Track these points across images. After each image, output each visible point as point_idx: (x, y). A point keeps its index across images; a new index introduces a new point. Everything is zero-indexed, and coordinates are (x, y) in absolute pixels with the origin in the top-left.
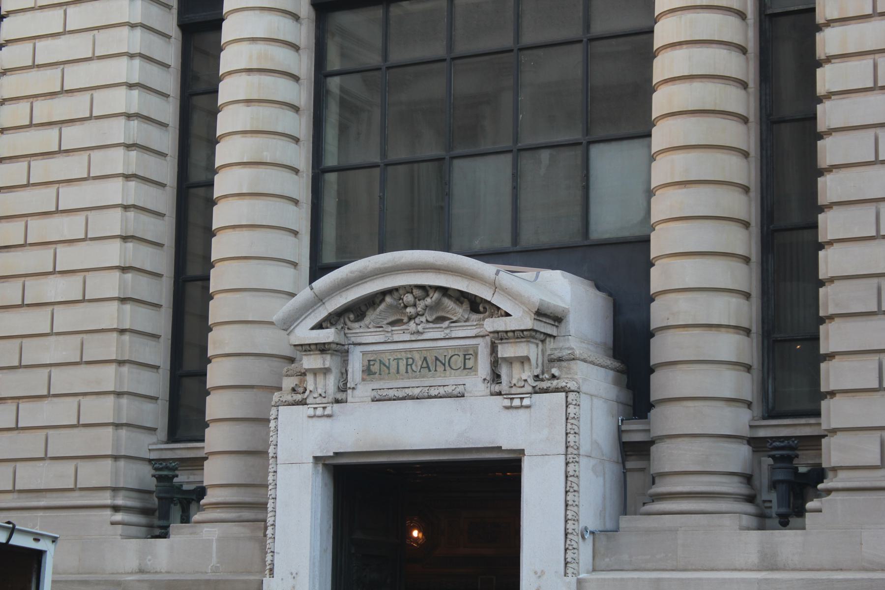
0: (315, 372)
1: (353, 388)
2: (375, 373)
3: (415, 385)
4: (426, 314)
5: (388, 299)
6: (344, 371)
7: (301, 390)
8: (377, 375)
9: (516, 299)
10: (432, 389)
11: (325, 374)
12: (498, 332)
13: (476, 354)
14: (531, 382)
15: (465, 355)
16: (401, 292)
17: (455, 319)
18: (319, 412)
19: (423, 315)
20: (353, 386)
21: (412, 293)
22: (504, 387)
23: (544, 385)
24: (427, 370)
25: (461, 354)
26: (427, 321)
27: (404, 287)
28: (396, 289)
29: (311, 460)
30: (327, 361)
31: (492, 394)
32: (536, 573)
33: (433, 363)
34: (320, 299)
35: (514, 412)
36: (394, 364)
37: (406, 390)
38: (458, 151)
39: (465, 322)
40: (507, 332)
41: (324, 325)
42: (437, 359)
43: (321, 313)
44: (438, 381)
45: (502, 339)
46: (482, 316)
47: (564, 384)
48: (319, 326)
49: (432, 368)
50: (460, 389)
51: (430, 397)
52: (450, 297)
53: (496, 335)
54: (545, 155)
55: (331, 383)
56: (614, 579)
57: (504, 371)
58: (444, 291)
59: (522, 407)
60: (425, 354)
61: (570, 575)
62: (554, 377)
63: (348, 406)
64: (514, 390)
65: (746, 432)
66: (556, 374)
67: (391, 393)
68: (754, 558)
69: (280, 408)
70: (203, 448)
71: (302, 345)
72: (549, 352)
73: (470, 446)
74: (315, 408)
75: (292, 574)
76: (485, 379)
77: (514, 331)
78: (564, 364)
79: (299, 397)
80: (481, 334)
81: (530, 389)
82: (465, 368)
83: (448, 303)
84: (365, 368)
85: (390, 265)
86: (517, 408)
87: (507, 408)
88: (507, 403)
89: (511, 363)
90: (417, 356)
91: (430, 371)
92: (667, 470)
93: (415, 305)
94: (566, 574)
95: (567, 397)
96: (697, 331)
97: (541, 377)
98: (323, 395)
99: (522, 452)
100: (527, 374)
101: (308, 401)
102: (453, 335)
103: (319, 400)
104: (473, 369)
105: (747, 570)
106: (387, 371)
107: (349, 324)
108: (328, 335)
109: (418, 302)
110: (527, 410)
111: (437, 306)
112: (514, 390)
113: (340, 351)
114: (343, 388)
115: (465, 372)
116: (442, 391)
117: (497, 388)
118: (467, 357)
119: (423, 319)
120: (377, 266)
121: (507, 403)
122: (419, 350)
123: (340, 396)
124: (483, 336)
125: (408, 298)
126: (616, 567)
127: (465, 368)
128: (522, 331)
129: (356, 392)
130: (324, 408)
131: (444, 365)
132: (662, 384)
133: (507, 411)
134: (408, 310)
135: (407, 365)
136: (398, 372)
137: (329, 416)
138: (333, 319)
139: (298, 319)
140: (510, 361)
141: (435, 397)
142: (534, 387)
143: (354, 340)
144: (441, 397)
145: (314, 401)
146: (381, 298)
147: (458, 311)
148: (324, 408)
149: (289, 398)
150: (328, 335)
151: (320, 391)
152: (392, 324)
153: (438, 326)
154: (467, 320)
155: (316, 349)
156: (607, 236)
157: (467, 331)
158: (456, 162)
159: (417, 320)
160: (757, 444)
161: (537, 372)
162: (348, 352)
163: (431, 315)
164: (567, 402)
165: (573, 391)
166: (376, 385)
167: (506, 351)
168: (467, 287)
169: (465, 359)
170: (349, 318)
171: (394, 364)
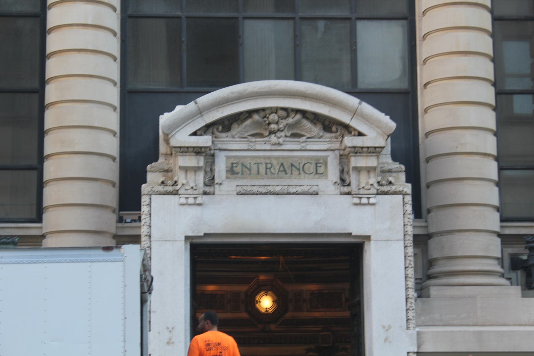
0: (186, 169)
1: (220, 184)
2: (238, 173)
3: (276, 184)
4: (286, 130)
5: (256, 117)
6: (208, 169)
7: (170, 182)
8: (239, 175)
9: (372, 124)
10: (291, 187)
11: (195, 171)
12: (355, 147)
13: (326, 164)
14: (376, 185)
15: (317, 164)
16: (268, 112)
17: (308, 136)
18: (191, 201)
19: (282, 131)
21: (276, 113)
22: (354, 188)
23: (385, 189)
24: (284, 173)
25: (313, 162)
26: (286, 136)
27: (271, 108)
28: (263, 110)
29: (183, 239)
30: (201, 161)
31: (341, 194)
32: (384, 327)
33: (288, 168)
34: (200, 112)
35: (362, 207)
36: (254, 168)
37: (268, 187)
38: (249, 14)
39: (319, 138)
40: (362, 148)
41: (199, 133)
42: (292, 165)
43: (200, 123)
44: (295, 182)
45: (356, 153)
46: (334, 135)
47: (401, 189)
48: (195, 134)
49: (289, 172)
50: (315, 189)
51: (289, 194)
52: (307, 118)
53: (353, 149)
54: (321, 24)
55: (201, 177)
56: (445, 332)
57: (353, 178)
58: (304, 113)
59: (369, 204)
60: (281, 161)
61: (412, 329)
62: (390, 183)
63: (216, 198)
64: (362, 191)
65: (497, 229)
66: (393, 181)
67: (255, 189)
69: (153, 197)
70: (41, 228)
71: (180, 147)
72: (381, 166)
73: (322, 232)
74: (187, 198)
75: (168, 328)
76: (335, 183)
77: (368, 148)
78: (394, 174)
79: (170, 189)
80: (332, 148)
81: (375, 191)
82: (316, 173)
83: (307, 124)
84: (229, 169)
85: (266, 90)
86: (364, 205)
87: (356, 204)
88: (356, 201)
89: (359, 171)
90: (275, 162)
91: (286, 174)
92: (458, 254)
93: (277, 123)
94: (408, 328)
95: (404, 198)
96: (478, 157)
97: (381, 183)
98: (195, 188)
99: (368, 238)
100: (373, 180)
101: (180, 192)
102: (309, 147)
103: (190, 192)
104: (324, 175)
105: (530, 325)
106: (249, 172)
107: (217, 134)
108: (205, 141)
109: (281, 121)
110: (372, 207)
112: (362, 191)
114: (211, 182)
115: (317, 176)
116: (299, 189)
117: (346, 189)
118: (318, 165)
119: (283, 134)
120: (255, 90)
121: (356, 201)
122: (277, 158)
123: (207, 189)
124: (332, 150)
125: (273, 117)
126: (430, 323)
127: (316, 173)
128: (375, 148)
129: (222, 187)
130: (195, 198)
131: (299, 170)
133: (355, 207)
134: (273, 126)
135: (266, 168)
136: (258, 173)
137: (200, 205)
138: (207, 129)
139: (179, 126)
140: (358, 170)
141: (293, 194)
142: (378, 190)
143: (220, 146)
144: (298, 194)
145: (186, 192)
146: (247, 115)
147: (316, 130)
148: (195, 198)
149: (161, 188)
150: (205, 141)
151: (192, 184)
152: (253, 135)
153: (296, 140)
154: (321, 137)
155: (193, 152)
156: (372, 87)
157: (321, 145)
158: (247, 22)
159: (279, 134)
160: (506, 240)
161: (379, 179)
162: (213, 155)
163: (288, 131)
164: (404, 202)
165: (408, 194)
166: (240, 182)
168: (329, 111)
169: (317, 167)
170: (217, 129)
171: (254, 168)
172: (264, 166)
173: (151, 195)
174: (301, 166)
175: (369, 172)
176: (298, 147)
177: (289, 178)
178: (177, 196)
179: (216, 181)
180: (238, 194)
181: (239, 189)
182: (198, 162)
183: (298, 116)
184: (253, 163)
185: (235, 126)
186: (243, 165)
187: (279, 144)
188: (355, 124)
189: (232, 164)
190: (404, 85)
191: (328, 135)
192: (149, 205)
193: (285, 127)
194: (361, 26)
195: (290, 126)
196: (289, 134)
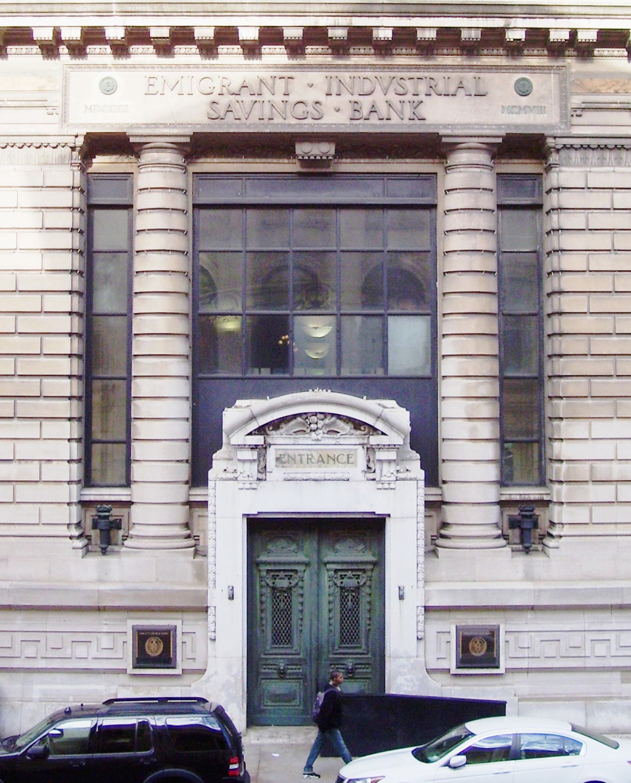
1: (271, 472)
5: (299, 419)
15: (348, 455)
16: (309, 415)
17: (342, 433)
18: (248, 486)
20: (271, 471)
26: (324, 433)
28: (305, 413)
30: (254, 455)
31: (368, 480)
39: (350, 435)
41: (253, 433)
42: (329, 456)
43: (254, 426)
45: (380, 449)
52: (341, 419)
53: (377, 446)
55: (255, 467)
58: (339, 416)
68: (521, 574)
71: (239, 445)
88: (380, 486)
91: (324, 462)
93: (316, 423)
95: (417, 484)
98: (250, 476)
102: (342, 442)
108: (258, 440)
111: (333, 423)
112: (384, 478)
113: (260, 449)
117: (371, 476)
119: (321, 431)
123: (260, 476)
125: (314, 419)
127: (348, 463)
131: (334, 460)
132: (446, 471)
135: (308, 459)
138: (261, 430)
147: (347, 428)
149: (224, 475)
163: (325, 429)
166: (288, 470)
167: (381, 455)
171: (298, 458)
172: (306, 456)
173: (215, 481)
174: (336, 456)
175: (390, 462)
176: (334, 442)
177: (325, 467)
178: (236, 482)
179: (268, 470)
180: (285, 480)
181: (286, 476)
182: (253, 456)
183: (334, 419)
184: (297, 454)
185: (283, 425)
186: (289, 456)
187: (318, 440)
188: (379, 426)
189: (281, 455)
190: (427, 372)
191: (359, 432)
192: (215, 488)
193: (323, 426)
194: (391, 319)
195: (327, 425)
196: (326, 432)
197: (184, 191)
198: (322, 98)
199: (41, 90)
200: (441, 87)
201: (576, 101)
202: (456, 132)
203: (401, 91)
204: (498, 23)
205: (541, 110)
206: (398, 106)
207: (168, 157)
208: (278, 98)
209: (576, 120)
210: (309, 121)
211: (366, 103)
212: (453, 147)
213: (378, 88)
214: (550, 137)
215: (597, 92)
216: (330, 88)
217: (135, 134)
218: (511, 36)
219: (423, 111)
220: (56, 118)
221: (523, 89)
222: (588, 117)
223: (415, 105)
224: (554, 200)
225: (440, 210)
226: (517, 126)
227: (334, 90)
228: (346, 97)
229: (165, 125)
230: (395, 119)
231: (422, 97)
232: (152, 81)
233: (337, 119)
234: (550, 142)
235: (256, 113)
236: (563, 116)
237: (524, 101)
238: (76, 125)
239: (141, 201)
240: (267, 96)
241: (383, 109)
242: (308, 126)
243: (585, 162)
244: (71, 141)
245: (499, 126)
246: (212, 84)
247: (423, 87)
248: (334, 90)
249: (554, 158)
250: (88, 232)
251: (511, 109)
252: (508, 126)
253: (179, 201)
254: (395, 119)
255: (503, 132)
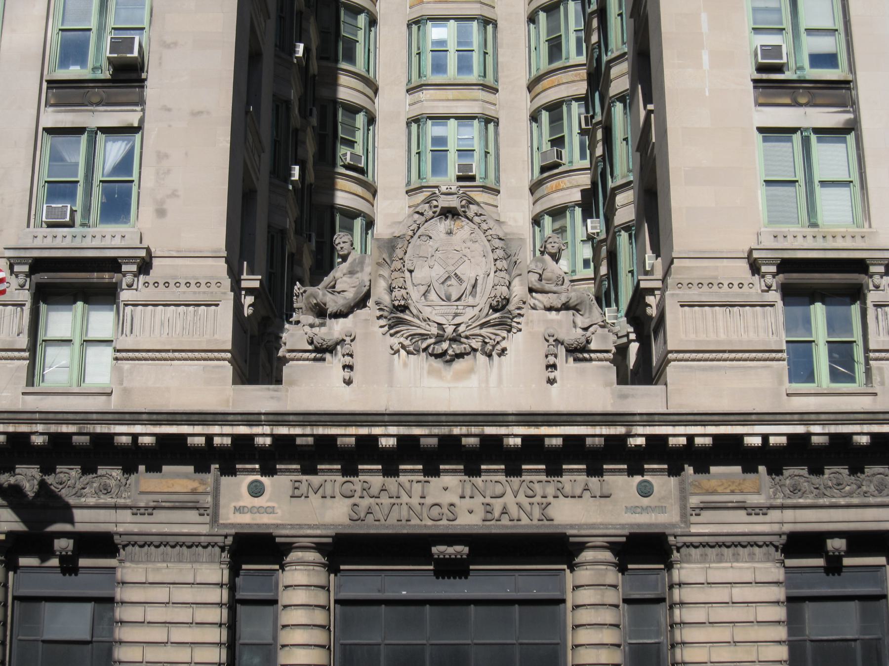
197: (325, 588)
198: (456, 500)
199: (194, 492)
200: (568, 489)
201: (694, 501)
202: (583, 532)
203: (530, 493)
204: (620, 430)
205: (662, 509)
206: (528, 508)
207: (313, 556)
208: (415, 501)
209: (694, 519)
210: (444, 522)
211: (497, 505)
212: (582, 547)
213: (509, 490)
214: (671, 535)
215: (714, 492)
216: (463, 492)
217: (282, 534)
218: (633, 442)
219: (551, 512)
220: (207, 519)
221: (645, 491)
222: (707, 515)
223: (543, 506)
224: (677, 594)
225: (569, 604)
226: (639, 525)
227: (468, 493)
228: (479, 499)
229: (310, 527)
230: (525, 520)
231: (550, 499)
232: (297, 484)
233: (470, 519)
234: (671, 539)
235: (394, 516)
236: (684, 516)
237: (645, 501)
238: (225, 526)
239: (286, 597)
240: (405, 498)
241: (514, 511)
242: (444, 526)
243: (704, 559)
244: (220, 540)
245: (623, 526)
246: (353, 487)
247: (550, 490)
248: (468, 493)
249: (676, 555)
250: (232, 626)
251: (633, 510)
252: (632, 525)
253: (320, 598)
254: (525, 520)
255: (626, 532)
